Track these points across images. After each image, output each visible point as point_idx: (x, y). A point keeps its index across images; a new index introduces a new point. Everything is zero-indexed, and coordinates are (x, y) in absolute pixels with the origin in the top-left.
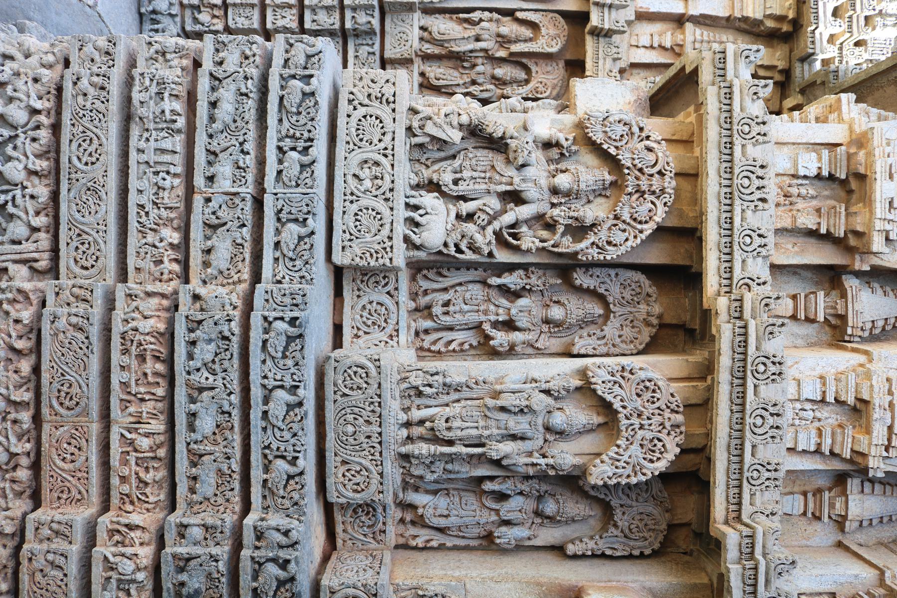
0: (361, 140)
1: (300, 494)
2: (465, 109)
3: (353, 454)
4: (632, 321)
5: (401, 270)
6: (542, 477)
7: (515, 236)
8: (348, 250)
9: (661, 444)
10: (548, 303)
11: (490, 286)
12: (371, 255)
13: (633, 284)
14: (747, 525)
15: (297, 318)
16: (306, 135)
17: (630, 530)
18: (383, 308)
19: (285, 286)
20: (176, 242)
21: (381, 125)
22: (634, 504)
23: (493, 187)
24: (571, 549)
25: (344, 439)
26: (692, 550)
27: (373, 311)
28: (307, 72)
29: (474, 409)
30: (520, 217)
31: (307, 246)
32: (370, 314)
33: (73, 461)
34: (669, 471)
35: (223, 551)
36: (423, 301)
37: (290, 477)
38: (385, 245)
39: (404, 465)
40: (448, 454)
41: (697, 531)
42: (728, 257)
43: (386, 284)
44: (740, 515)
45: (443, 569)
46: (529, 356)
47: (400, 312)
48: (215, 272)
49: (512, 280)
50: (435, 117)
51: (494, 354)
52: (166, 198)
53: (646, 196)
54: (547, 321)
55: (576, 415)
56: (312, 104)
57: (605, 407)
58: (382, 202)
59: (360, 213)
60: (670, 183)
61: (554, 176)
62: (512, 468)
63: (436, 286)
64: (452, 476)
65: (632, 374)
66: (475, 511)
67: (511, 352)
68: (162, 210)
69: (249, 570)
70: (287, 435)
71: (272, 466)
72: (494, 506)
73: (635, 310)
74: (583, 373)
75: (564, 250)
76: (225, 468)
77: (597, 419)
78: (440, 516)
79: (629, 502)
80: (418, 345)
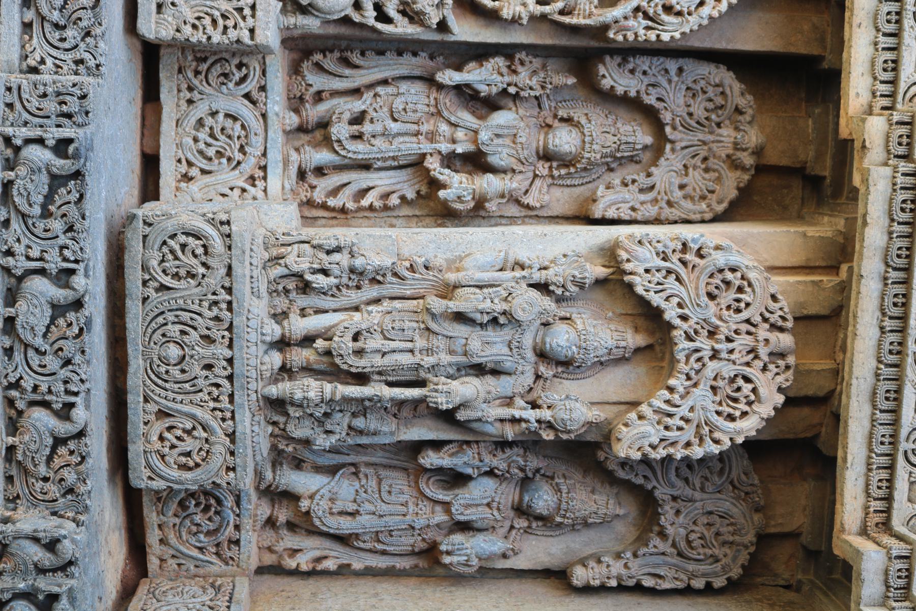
1: (78, 473)
3: (179, 398)
4: (705, 159)
5: (271, 52)
6: (530, 443)
9: (750, 386)
10: (549, 121)
11: (440, 87)
12: (214, 22)
13: (710, 89)
14: (900, 538)
15: (70, 141)
17: (689, 542)
18: (238, 126)
19: (46, 78)
22: (698, 495)
24: (580, 576)
25: (163, 369)
26: (800, 581)
27: (217, 131)
29: (406, 316)
32: (212, 135)
34: (762, 437)
36: (314, 113)
37: (59, 441)
39: (275, 419)
40: (356, 400)
41: (812, 548)
42: (891, 42)
43: (243, 80)
44: (889, 519)
46: (512, 220)
49: (484, 76)
51: (447, 215)
54: (546, 156)
55: (596, 330)
57: (650, 317)
62: (475, 425)
64: (364, 440)
65: (702, 257)
66: (405, 504)
67: (478, 212)
70: (52, 363)
71: (23, 421)
72: (441, 496)
73: (710, 138)
74: (610, 254)
75: (582, 21)
77: (634, 340)
78: (341, 513)
79: (688, 492)
80: (304, 195)
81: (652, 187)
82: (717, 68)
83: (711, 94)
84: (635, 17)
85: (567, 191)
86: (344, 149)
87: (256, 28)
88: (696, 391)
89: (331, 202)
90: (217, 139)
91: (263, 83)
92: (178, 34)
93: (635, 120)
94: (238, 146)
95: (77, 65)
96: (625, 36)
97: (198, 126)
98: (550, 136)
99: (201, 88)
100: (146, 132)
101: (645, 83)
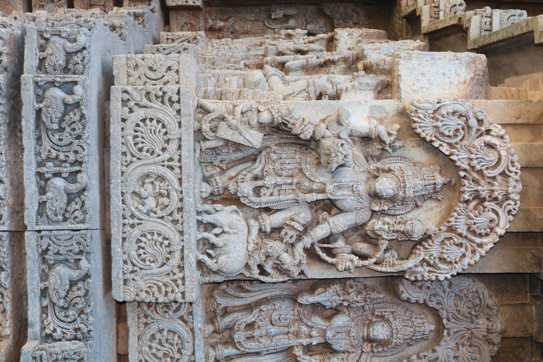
0: (141, 150)
2: (266, 104)
4: (469, 338)
7: (330, 252)
8: (132, 284)
10: (370, 317)
12: (159, 288)
16: (72, 157)
18: (176, 338)
21: (164, 131)
23: (302, 196)
27: (163, 341)
28: (70, 77)
30: (334, 231)
31: (81, 293)
32: (160, 344)
38: (175, 277)
47: (197, 341)
50: (230, 118)
53: (486, 204)
54: (369, 340)
56: (77, 118)
58: (170, 225)
59: (143, 239)
60: (515, 187)
61: (376, 177)
63: (237, 303)
73: (472, 326)
82: (474, 281)
83: (470, 298)
84: (422, 265)
85: (383, 359)
86: (243, 347)
87: (186, 292)
90: (164, 346)
91: (191, 310)
92: (137, 297)
93: (423, 313)
94: (176, 350)
95: (76, 332)
96: (416, 277)
97: (151, 338)
98: (371, 329)
99: (153, 316)
100: (120, 342)
101: (429, 295)
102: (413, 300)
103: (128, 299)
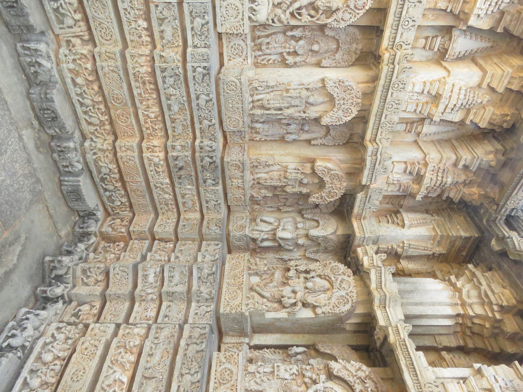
7: (300, 14)
8: (224, 26)
12: (234, 28)
14: (377, 144)
20: (146, 27)
30: (302, 5)
31: (206, 29)
32: (235, 49)
33: (126, 122)
35: (189, 153)
37: (209, 126)
45: (266, 150)
48: (167, 42)
49: (297, 33)
51: (287, 66)
52: (136, 4)
54: (311, 51)
68: (136, 10)
69: (199, 160)
70: (207, 112)
73: (350, 47)
76: (185, 123)
81: (335, 59)
88: (339, 112)
89: (262, 63)
102: (330, 35)
103: (223, 32)
